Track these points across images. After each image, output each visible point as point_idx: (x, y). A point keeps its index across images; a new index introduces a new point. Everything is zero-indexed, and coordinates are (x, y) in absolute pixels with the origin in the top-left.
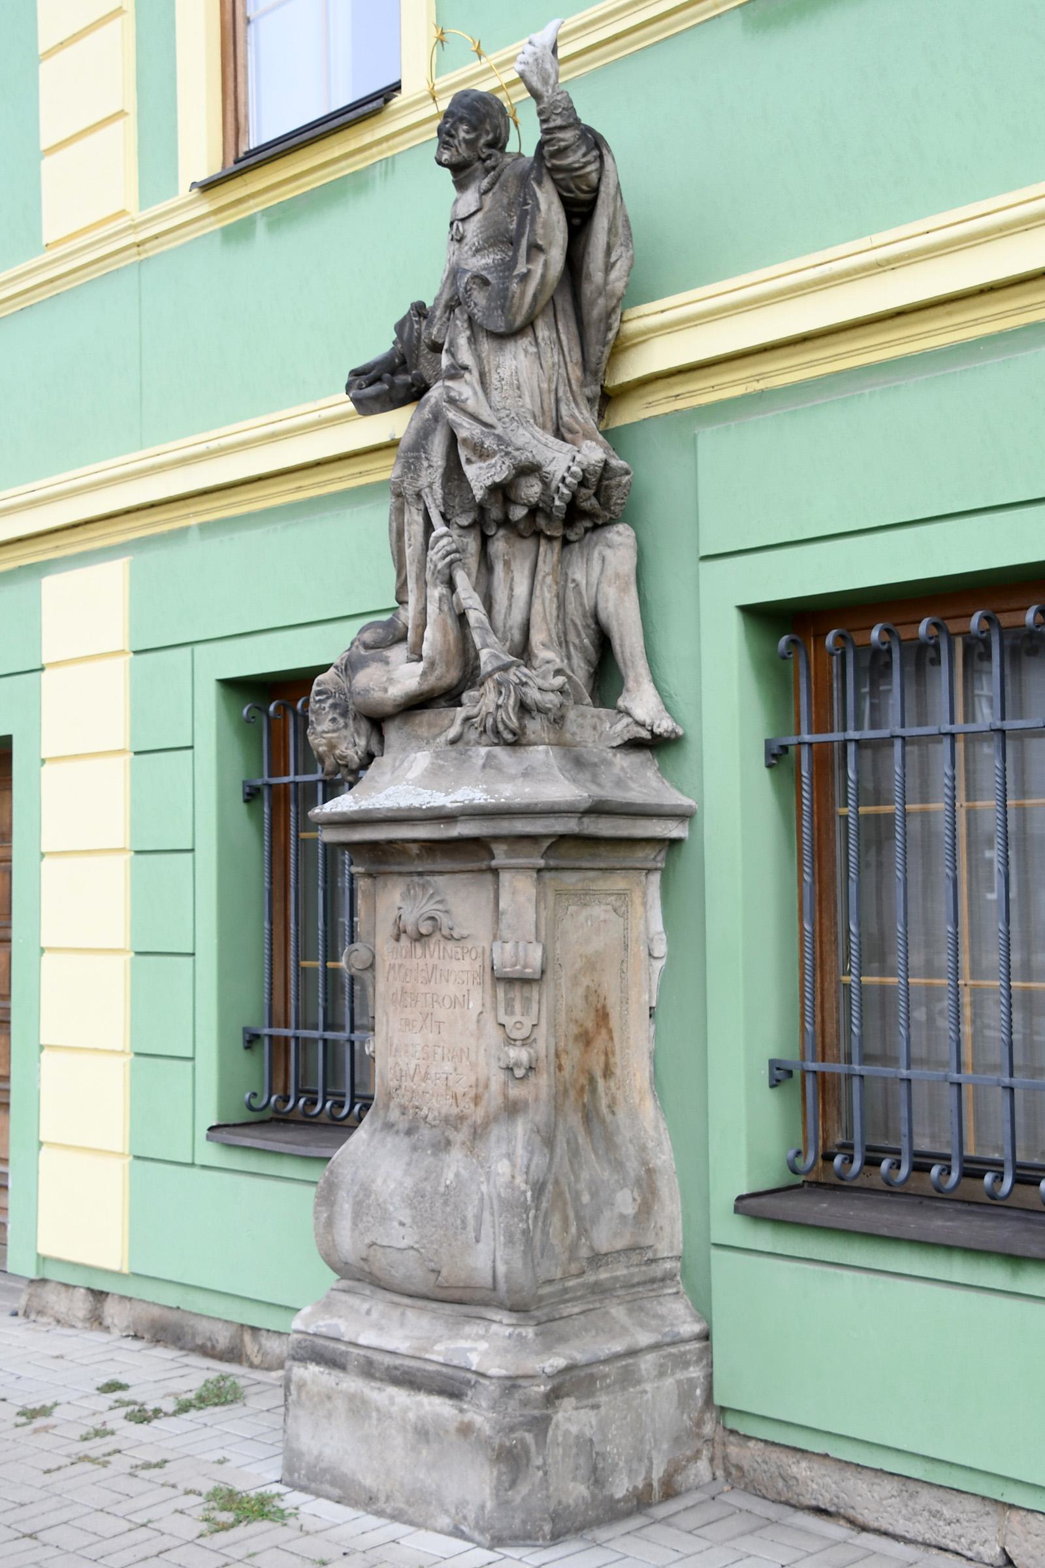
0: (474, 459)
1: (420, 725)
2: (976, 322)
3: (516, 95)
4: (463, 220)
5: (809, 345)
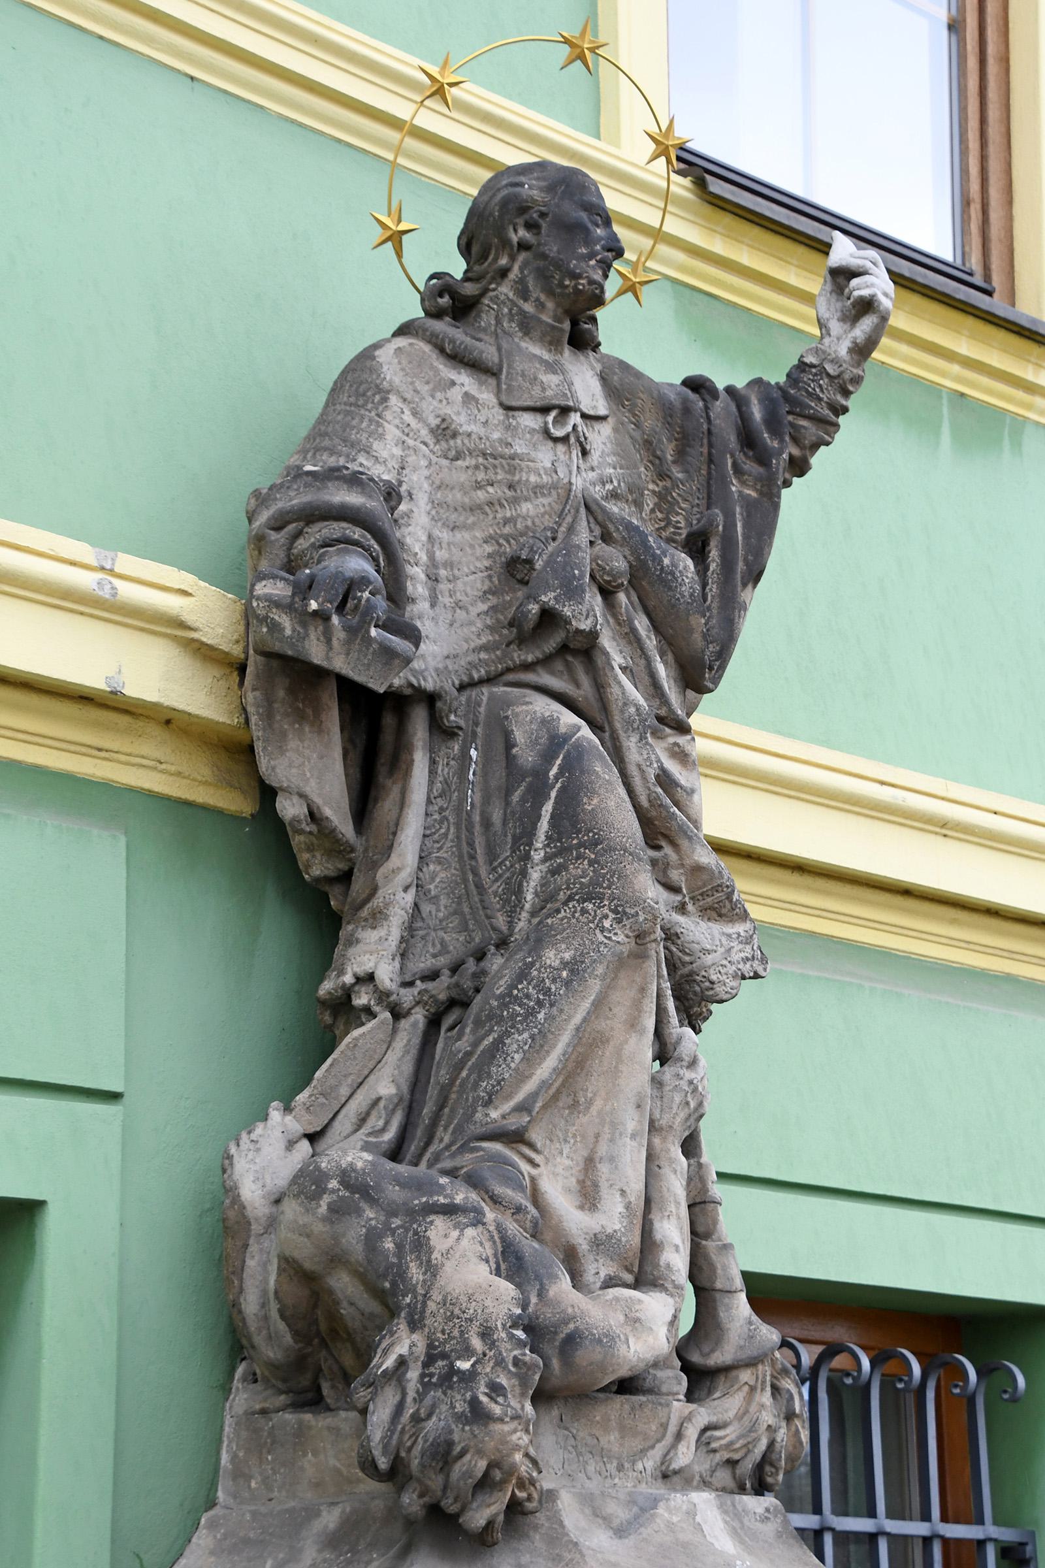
0: (690, 907)
1: (605, 1426)
2: (968, 945)
3: (410, 156)
4: (584, 416)
5: (808, 880)
